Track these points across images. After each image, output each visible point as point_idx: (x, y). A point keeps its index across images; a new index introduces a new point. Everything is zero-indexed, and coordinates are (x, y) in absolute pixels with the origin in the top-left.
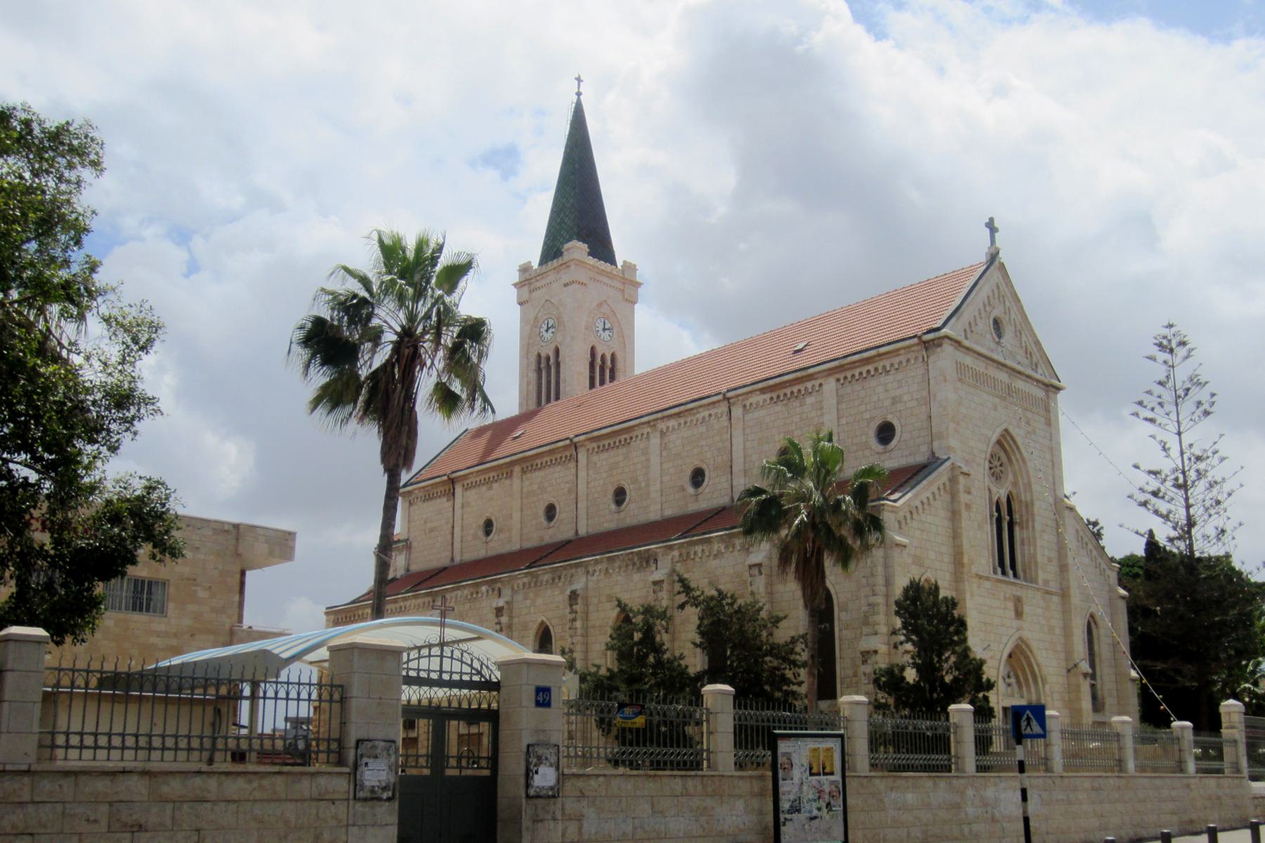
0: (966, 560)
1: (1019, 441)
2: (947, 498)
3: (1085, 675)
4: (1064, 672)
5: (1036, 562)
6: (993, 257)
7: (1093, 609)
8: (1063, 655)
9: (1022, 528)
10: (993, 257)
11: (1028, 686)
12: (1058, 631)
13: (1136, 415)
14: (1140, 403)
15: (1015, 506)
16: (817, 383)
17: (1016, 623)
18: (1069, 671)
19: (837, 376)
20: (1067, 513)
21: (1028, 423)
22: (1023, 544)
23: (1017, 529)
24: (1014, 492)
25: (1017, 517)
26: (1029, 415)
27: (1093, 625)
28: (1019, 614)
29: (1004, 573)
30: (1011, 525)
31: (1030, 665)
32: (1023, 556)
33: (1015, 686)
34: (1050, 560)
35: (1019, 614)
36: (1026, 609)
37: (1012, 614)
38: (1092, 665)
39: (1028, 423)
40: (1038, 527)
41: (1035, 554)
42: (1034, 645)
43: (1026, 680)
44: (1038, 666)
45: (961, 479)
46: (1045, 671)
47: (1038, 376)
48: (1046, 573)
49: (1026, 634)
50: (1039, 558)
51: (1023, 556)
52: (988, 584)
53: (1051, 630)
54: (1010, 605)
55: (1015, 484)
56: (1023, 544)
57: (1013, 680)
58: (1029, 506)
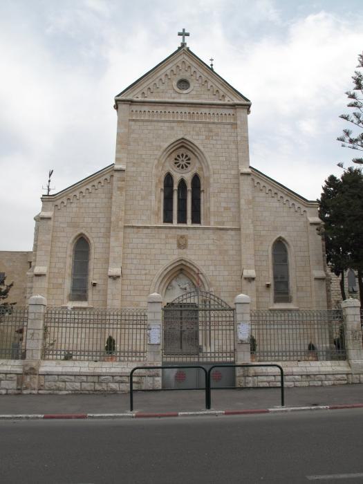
0: (113, 219)
6: (183, 45)
10: (183, 45)
17: (176, 252)
24: (200, 174)
37: (175, 246)
39: (211, 131)
41: (209, 208)
47: (226, 102)
50: (212, 209)
55: (201, 169)
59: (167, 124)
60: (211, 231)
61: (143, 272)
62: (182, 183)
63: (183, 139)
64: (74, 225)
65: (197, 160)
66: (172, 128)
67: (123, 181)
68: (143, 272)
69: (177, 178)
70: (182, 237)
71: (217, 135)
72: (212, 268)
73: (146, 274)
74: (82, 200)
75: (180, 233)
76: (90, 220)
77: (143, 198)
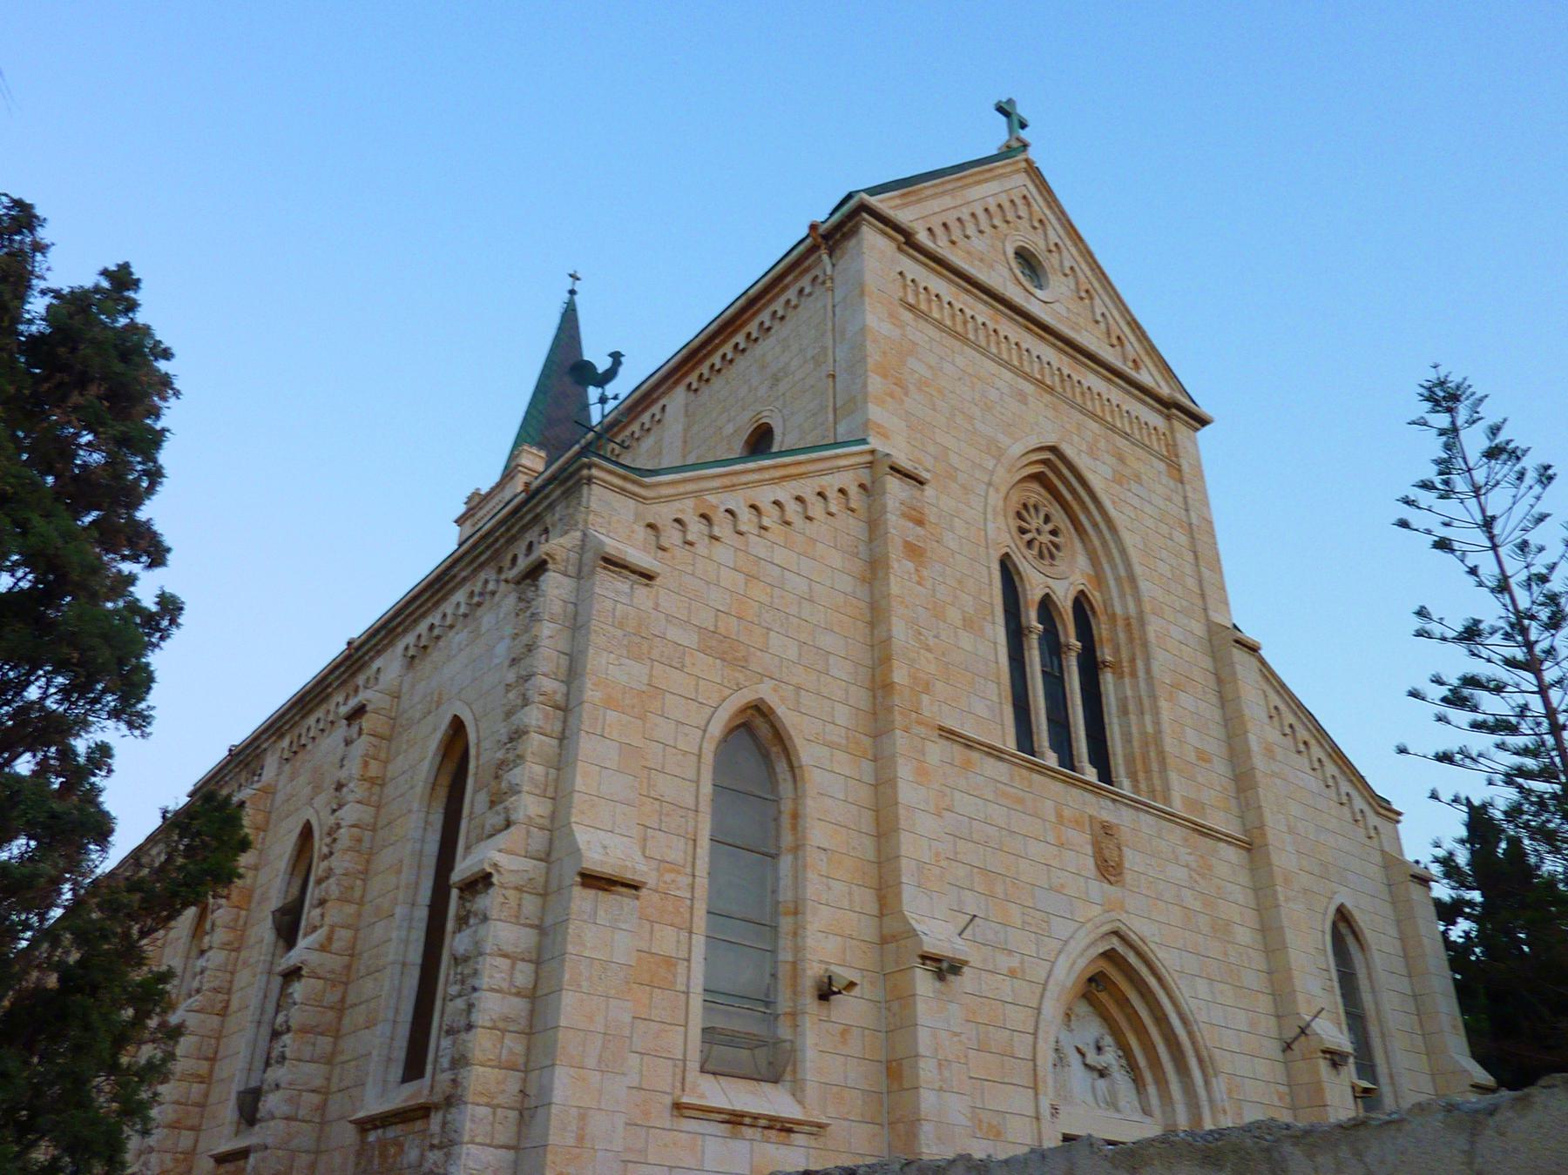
0: (900, 676)
1: (1082, 462)
2: (854, 527)
3: (1335, 1059)
4: (1273, 1049)
5: (1162, 756)
7: (1345, 897)
8: (1264, 1003)
9: (1119, 675)
11: (1162, 1082)
12: (1244, 935)
13: (1404, 524)
14: (1408, 502)
15: (1101, 629)
16: (656, 409)
17: (1097, 889)
18: (1288, 1047)
19: (687, 380)
20: (1239, 655)
21: (1121, 459)
22: (1124, 712)
23: (1108, 680)
24: (1096, 597)
25: (1106, 653)
26: (1121, 443)
27: (1350, 940)
28: (1109, 869)
29: (1067, 759)
30: (1091, 668)
31: (1161, 1020)
32: (1127, 739)
33: (1121, 1080)
34: (1203, 756)
35: (1109, 869)
36: (1133, 860)
38: (1356, 1019)
39: (1121, 459)
40: (1161, 662)
42: (1166, 958)
43: (1155, 1063)
44: (1185, 1021)
45: (893, 484)
46: (1207, 1036)
48: (1198, 786)
49: (1141, 927)
51: (1127, 739)
52: (991, 767)
53: (1221, 930)
54: (1082, 840)
56: (1124, 712)
57: (1110, 1057)
58: (1135, 627)
59: (1007, 375)
60: (1179, 831)
61: (1005, 963)
62: (1047, 606)
63: (1053, 449)
64: (725, 649)
65: (1078, 545)
66: (1022, 398)
67: (920, 523)
68: (1005, 963)
69: (1035, 584)
70: (1107, 830)
71: (1138, 479)
72: (1202, 987)
73: (1012, 974)
74: (758, 546)
75: (1105, 811)
76: (792, 653)
77: (968, 624)
